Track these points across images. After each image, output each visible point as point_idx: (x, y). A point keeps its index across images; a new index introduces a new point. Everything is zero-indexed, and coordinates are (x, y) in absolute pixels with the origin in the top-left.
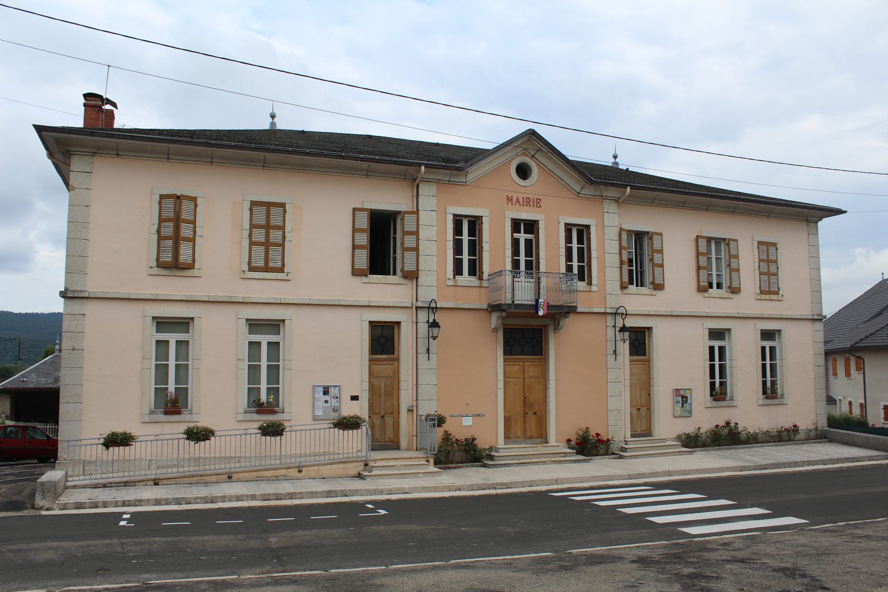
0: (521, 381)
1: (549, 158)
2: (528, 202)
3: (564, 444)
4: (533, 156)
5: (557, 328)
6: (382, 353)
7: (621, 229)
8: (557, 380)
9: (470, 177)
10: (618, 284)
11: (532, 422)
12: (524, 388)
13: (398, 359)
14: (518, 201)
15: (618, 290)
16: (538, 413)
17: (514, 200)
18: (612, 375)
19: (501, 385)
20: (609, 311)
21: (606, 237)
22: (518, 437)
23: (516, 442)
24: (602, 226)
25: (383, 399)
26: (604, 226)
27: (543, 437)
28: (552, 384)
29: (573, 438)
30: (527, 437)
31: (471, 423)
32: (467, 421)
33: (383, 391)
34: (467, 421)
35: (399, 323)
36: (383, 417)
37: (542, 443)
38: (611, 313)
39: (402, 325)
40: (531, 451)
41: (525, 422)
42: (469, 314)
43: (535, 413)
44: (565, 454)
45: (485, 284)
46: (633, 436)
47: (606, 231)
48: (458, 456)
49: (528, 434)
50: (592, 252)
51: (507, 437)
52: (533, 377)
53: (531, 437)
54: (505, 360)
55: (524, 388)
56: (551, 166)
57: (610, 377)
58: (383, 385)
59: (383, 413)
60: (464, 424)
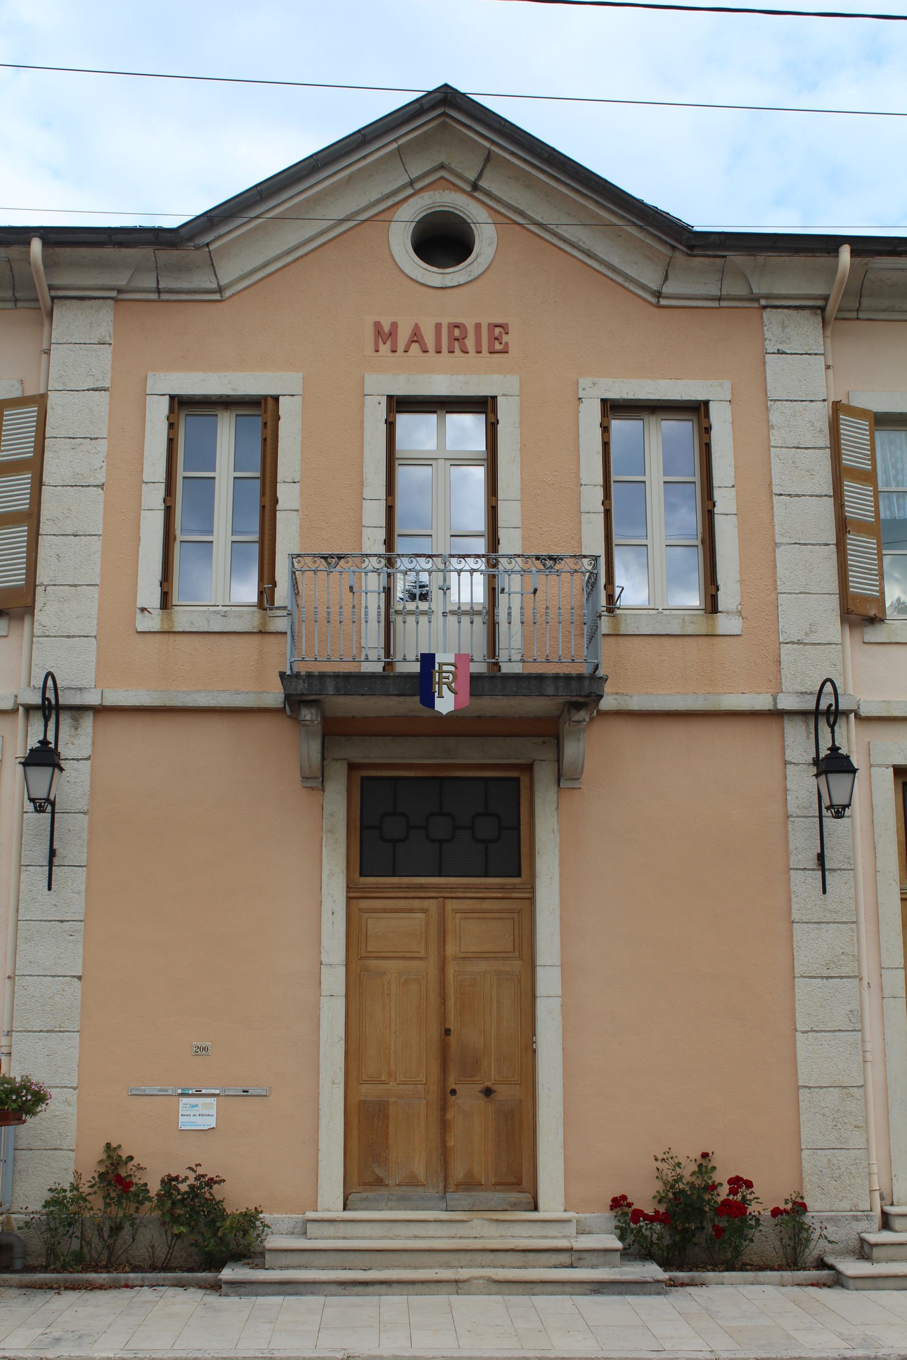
0: (431, 967)
1: (529, 183)
2: (456, 338)
3: (604, 1218)
4: (475, 187)
7: (837, 408)
8: (567, 968)
9: (229, 271)
10: (834, 602)
11: (472, 1120)
12: (443, 998)
14: (416, 337)
16: (502, 1092)
17: (403, 336)
18: (812, 948)
19: (334, 980)
20: (786, 703)
21: (776, 438)
22: (412, 1182)
23: (404, 1202)
24: (758, 401)
26: (766, 402)
27: (516, 1181)
28: (548, 981)
29: (645, 1199)
30: (450, 1184)
31: (211, 1122)
32: (199, 1114)
34: (199, 1114)
37: (515, 1207)
38: (803, 714)
40: (441, 1238)
41: (444, 1126)
42: (218, 728)
43: (488, 1092)
44: (576, 1256)
45: (281, 624)
47: (775, 417)
48: (150, 1236)
49: (458, 1172)
50: (717, 495)
51: (367, 1174)
53: (470, 1184)
54: (353, 894)
55: (443, 998)
56: (542, 212)
57: (801, 958)
60: (185, 1123)
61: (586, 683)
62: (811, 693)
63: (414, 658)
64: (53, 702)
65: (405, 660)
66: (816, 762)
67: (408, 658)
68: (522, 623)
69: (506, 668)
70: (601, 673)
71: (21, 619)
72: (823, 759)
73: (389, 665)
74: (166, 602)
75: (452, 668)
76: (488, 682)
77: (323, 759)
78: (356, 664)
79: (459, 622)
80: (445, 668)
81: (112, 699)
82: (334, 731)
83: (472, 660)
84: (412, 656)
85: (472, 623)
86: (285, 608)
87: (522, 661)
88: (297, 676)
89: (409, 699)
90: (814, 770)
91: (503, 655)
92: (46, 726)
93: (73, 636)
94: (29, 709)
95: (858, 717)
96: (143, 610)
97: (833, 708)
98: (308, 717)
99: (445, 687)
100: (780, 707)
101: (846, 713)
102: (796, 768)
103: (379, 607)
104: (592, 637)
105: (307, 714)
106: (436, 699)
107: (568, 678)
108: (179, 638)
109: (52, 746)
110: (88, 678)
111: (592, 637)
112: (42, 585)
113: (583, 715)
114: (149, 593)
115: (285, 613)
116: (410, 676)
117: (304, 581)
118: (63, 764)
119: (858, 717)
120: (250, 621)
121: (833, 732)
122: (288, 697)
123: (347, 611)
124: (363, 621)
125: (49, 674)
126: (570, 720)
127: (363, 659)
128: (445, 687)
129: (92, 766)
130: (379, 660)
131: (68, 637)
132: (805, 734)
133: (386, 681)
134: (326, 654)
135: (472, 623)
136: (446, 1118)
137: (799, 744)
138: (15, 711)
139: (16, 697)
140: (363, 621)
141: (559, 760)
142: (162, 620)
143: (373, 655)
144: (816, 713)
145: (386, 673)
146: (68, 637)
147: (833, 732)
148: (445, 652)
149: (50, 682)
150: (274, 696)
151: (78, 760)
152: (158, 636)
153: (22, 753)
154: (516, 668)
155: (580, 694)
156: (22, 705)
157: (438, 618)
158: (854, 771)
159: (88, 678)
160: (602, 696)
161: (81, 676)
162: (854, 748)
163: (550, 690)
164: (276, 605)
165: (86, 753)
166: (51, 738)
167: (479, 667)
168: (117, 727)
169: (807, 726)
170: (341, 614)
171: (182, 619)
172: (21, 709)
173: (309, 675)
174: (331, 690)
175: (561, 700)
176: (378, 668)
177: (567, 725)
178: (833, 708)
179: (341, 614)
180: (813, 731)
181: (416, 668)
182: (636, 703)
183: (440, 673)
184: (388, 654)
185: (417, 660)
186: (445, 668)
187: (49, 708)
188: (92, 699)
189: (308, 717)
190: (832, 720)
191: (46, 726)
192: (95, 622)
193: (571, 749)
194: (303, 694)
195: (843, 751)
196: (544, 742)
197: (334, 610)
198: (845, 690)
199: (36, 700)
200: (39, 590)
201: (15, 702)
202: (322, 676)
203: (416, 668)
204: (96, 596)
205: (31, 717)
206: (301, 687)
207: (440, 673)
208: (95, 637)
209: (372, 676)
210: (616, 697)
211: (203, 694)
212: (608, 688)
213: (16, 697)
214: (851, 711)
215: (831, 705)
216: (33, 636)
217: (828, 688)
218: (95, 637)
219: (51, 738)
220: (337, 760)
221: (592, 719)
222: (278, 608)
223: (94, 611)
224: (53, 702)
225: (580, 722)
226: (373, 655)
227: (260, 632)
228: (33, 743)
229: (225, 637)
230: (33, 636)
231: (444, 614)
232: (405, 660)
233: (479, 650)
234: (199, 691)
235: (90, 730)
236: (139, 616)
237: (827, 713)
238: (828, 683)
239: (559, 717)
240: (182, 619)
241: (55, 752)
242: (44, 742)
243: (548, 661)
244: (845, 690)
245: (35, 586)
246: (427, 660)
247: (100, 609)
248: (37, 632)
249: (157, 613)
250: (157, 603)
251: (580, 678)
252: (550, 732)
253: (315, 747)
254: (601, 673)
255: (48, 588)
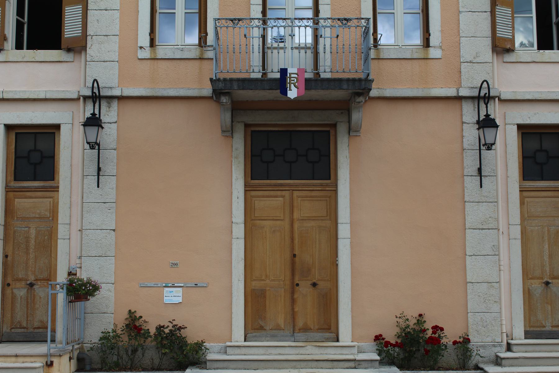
0: (286, 224)
3: (370, 345)
5: (353, 130)
6: (35, 179)
8: (353, 224)
10: (489, 42)
12: (292, 239)
13: (56, 189)
15: (487, 54)
16: (321, 284)
18: (474, 214)
19: (239, 230)
20: (464, 92)
22: (278, 328)
23: (274, 338)
25: (32, 256)
27: (328, 328)
29: (391, 335)
30: (296, 329)
31: (180, 300)
32: (173, 296)
33: (33, 242)
34: (173, 296)
35: (57, 127)
36: (31, 285)
37: (328, 340)
38: (472, 98)
39: (62, 127)
41: (293, 301)
42: (180, 108)
43: (314, 285)
45: (210, 54)
46: (528, 335)
49: (300, 323)
51: (255, 325)
52: (309, 219)
53: (306, 329)
54: (248, 188)
55: (292, 239)
57: (469, 219)
58: (33, 232)
59: (32, 278)
60: (167, 300)
61: (363, 83)
62: (476, 88)
63: (277, 71)
64: (97, 94)
65: (272, 72)
66: (478, 122)
67: (274, 71)
68: (331, 53)
69: (323, 76)
70: (370, 77)
71: (80, 53)
72: (482, 121)
73: (264, 74)
74: (152, 43)
75: (296, 76)
76: (314, 82)
77: (232, 122)
78: (248, 74)
79: (299, 53)
80: (292, 76)
81: (128, 92)
82: (237, 108)
83: (306, 72)
84: (276, 70)
85: (306, 53)
86: (212, 46)
87: (331, 72)
88: (219, 80)
89: (274, 91)
90: (477, 126)
91: (321, 69)
92: (94, 106)
93: (107, 61)
94: (85, 98)
95: (500, 100)
96: (141, 48)
97: (487, 95)
98: (224, 101)
99: (292, 85)
100: (460, 95)
101: (494, 98)
102: (468, 125)
103: (259, 45)
104: (366, 60)
105: (224, 99)
106: (289, 92)
107: (354, 80)
108: (159, 61)
109: (98, 116)
110: (114, 82)
111: (366, 60)
112: (90, 35)
113: (361, 99)
114: (144, 40)
115: (212, 48)
116: (275, 80)
117: (221, 32)
118: (103, 125)
119: (500, 100)
120: (194, 53)
121: (487, 107)
122: (214, 91)
123: (243, 47)
124: (251, 53)
125: (95, 80)
126: (355, 101)
127: (251, 71)
128: (292, 85)
129: (118, 126)
130: (259, 72)
131: (104, 61)
132: (473, 108)
133: (263, 82)
134: (233, 69)
135: (306, 53)
136: (295, 293)
137: (469, 113)
138: (78, 99)
139: (79, 92)
140: (251, 53)
141: (349, 122)
142: (151, 53)
143: (256, 70)
144: (478, 98)
145: (263, 78)
146: (104, 61)
147: (487, 107)
148: (292, 67)
149: (95, 85)
150: (207, 90)
151: (110, 123)
152: (149, 61)
153: (82, 120)
154: (328, 76)
155: (360, 88)
156: (82, 96)
157: (289, 51)
158: (497, 126)
159: (114, 82)
160: (371, 89)
161: (111, 82)
162: (497, 115)
163: (345, 86)
164: (208, 44)
165: (115, 119)
166: (97, 112)
167: (309, 75)
168: (131, 108)
169: (474, 104)
170: (240, 48)
171: (161, 52)
172: (81, 98)
173: (225, 80)
174: (235, 87)
175: (350, 91)
176: (259, 76)
177: (353, 104)
178: (487, 95)
179: (240, 48)
180: (477, 107)
181: (278, 76)
182: (388, 93)
183: (290, 78)
184: (264, 69)
185: (278, 72)
186: (292, 76)
187: (96, 97)
188: (117, 92)
189: (224, 101)
190: (486, 101)
191: (94, 106)
192: (117, 54)
193: (355, 116)
194: (222, 89)
195: (492, 117)
196: (342, 113)
197: (237, 47)
198: (493, 86)
199: (88, 93)
200: (89, 38)
201: (79, 94)
202: (231, 80)
203: (278, 76)
204: (117, 41)
205: (87, 102)
206: (221, 85)
207: (290, 78)
208: (117, 61)
209: (256, 80)
210: (378, 90)
211: (172, 90)
212: (374, 85)
213: (79, 92)
214: (496, 97)
215: (486, 94)
216: (86, 61)
217: (485, 85)
218: (117, 61)
219: (97, 112)
220: (239, 122)
221: (366, 101)
222: (209, 46)
223: (117, 49)
224: (97, 94)
225: (359, 102)
226: (256, 70)
227: (200, 59)
228: (88, 115)
229: (183, 61)
230: (86, 61)
231: (292, 48)
232: (272, 72)
233: (309, 67)
234: (170, 88)
235: (116, 108)
236: (139, 51)
237: (484, 98)
238: (485, 83)
239: (349, 100)
240: (161, 52)
241: (99, 119)
242: (94, 114)
243: (344, 72)
244: (493, 86)
245: (87, 36)
246: (284, 72)
247: (119, 47)
248: (88, 59)
249: (148, 49)
250: (148, 44)
251: (360, 80)
252: (345, 108)
253: (228, 115)
254: (370, 77)
255: (93, 37)
